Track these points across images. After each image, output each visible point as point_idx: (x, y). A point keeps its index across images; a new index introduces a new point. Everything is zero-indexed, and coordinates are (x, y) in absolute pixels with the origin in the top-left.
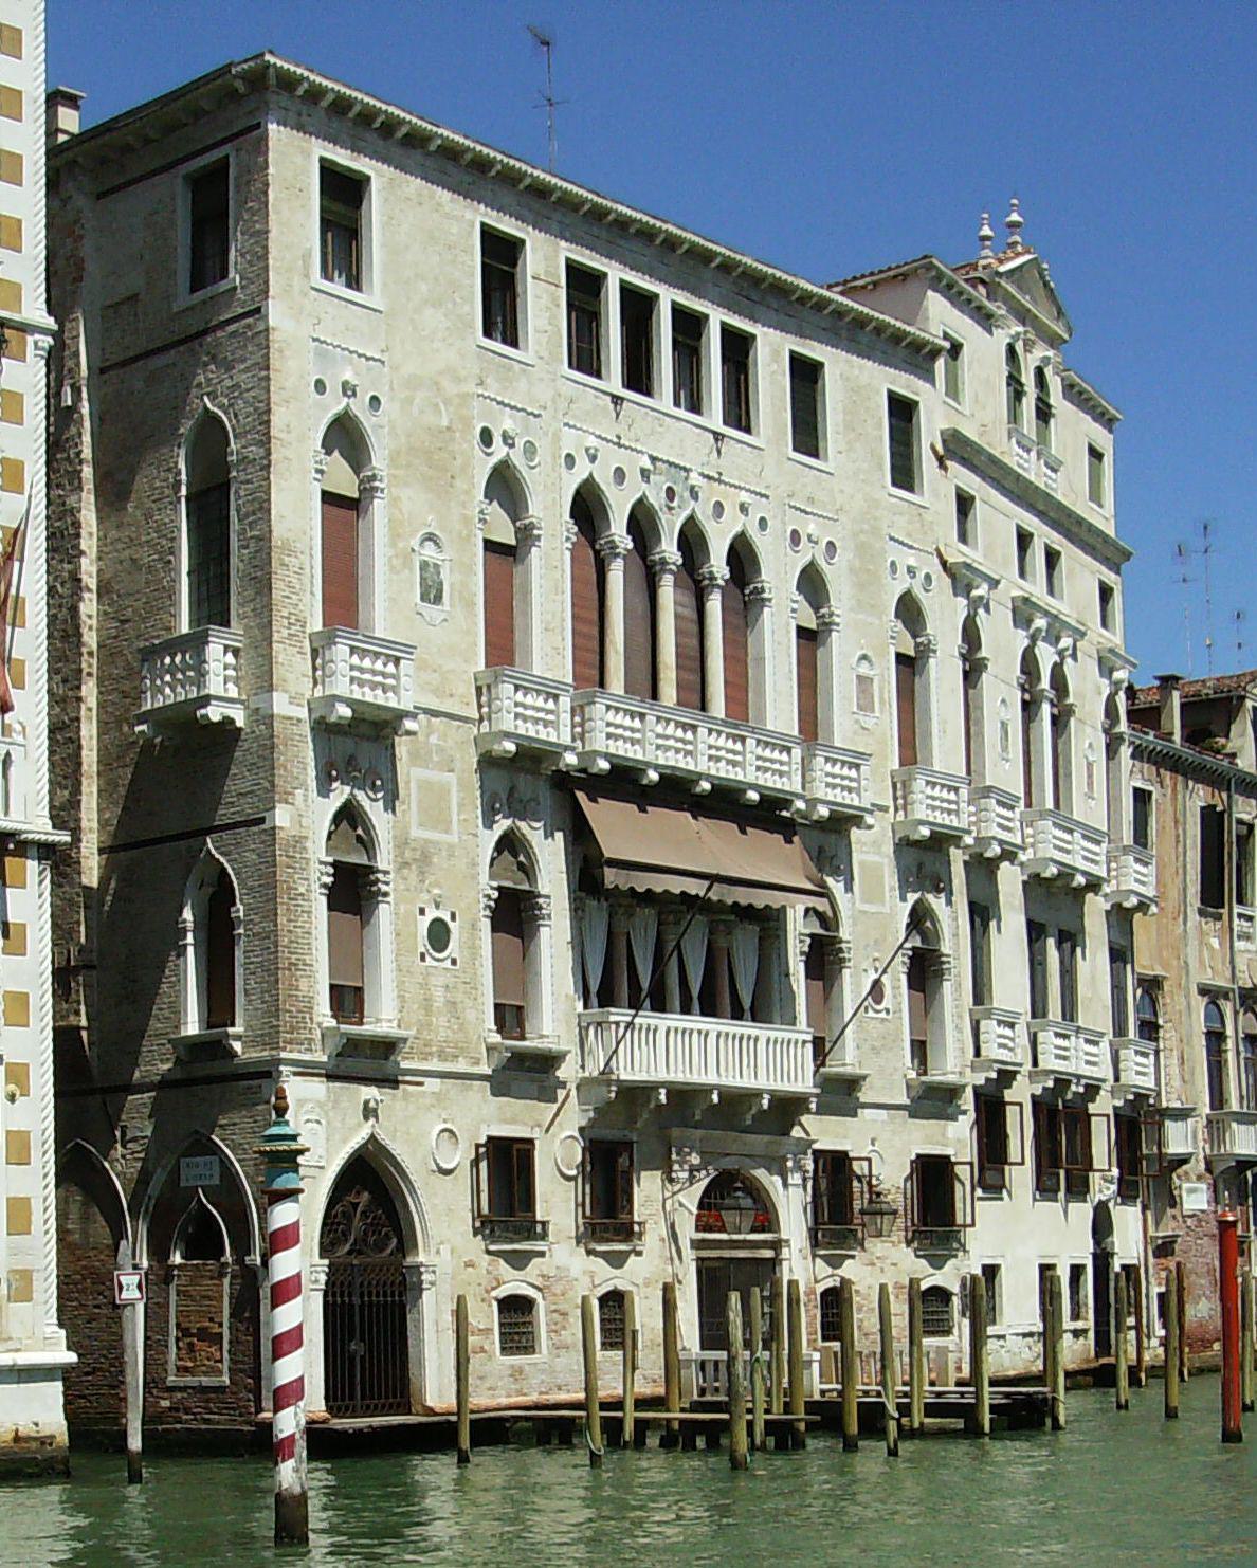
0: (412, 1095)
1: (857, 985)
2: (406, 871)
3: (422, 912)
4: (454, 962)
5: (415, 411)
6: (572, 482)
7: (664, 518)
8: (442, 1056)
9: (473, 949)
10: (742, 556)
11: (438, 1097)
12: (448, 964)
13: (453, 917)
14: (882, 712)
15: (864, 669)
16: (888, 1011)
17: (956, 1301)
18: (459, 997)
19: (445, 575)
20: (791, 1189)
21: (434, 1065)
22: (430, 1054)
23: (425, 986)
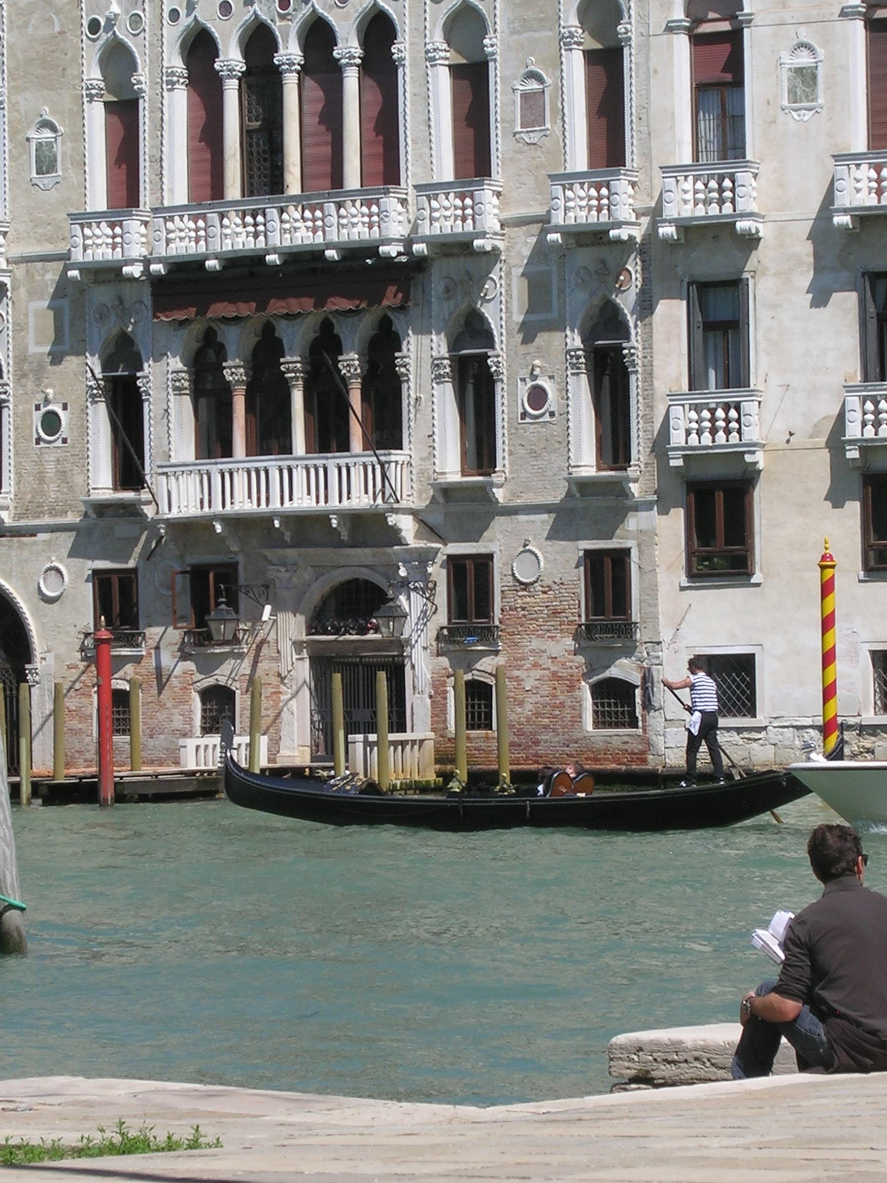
0: (25, 544)
1: (513, 395)
2: (24, 381)
3: (38, 408)
4: (65, 441)
5: (30, 31)
6: (172, 36)
7: (277, 27)
8: (52, 513)
9: (83, 430)
10: (378, 30)
11: (47, 543)
12: (59, 443)
13: (65, 407)
14: (553, 122)
15: (534, 85)
16: (552, 414)
17: (638, 692)
18: (68, 466)
19: (58, 149)
20: (413, 594)
21: (47, 520)
22: (42, 512)
23: (39, 463)
